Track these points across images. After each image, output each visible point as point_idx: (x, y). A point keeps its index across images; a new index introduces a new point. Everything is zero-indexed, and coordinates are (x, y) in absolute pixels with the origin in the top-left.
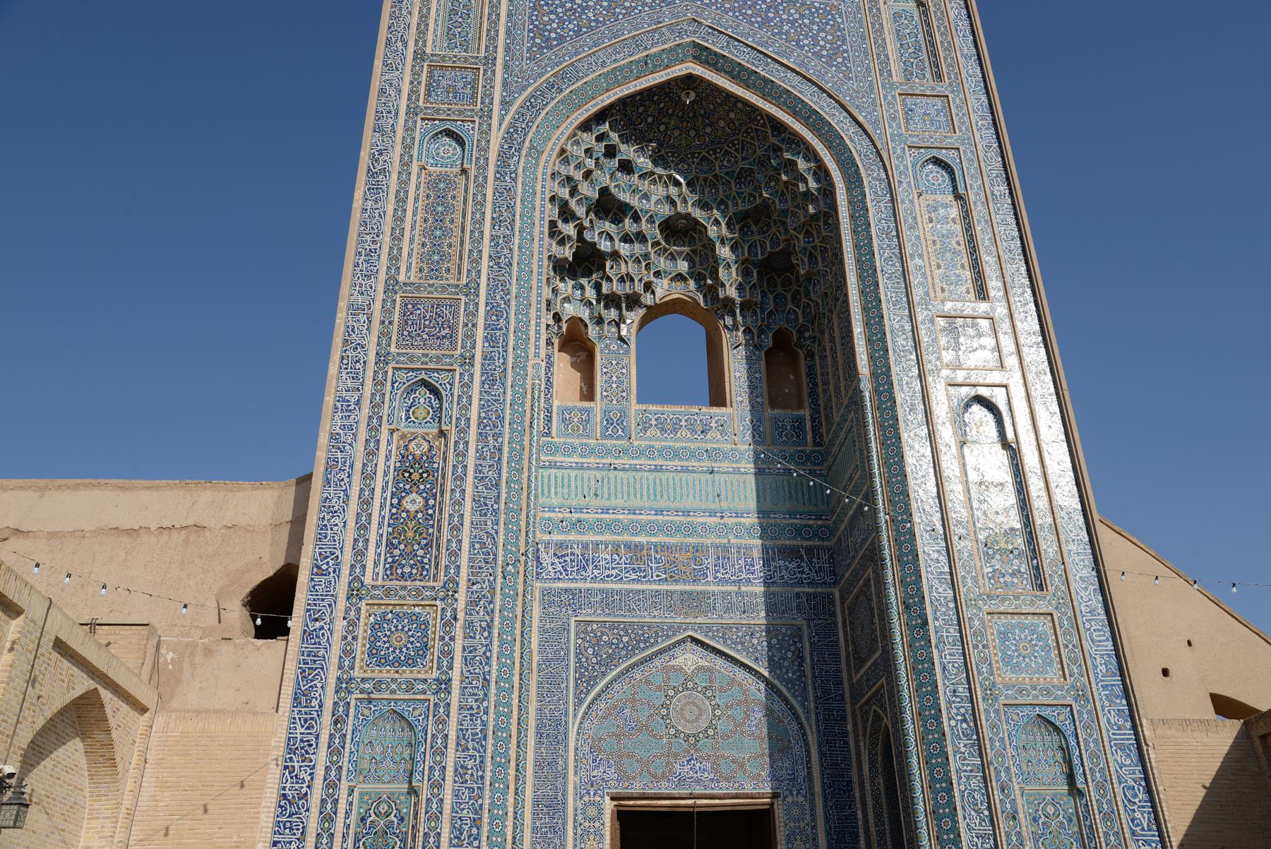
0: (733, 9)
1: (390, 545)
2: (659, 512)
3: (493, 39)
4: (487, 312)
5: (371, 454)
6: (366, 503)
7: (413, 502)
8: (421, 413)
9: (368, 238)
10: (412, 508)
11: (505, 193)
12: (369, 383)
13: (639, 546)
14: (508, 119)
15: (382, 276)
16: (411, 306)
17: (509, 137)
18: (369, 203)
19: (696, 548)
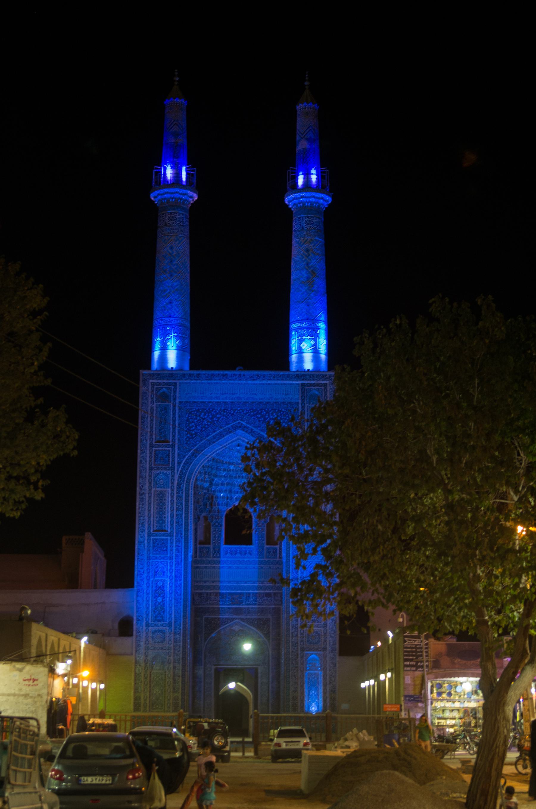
0: (254, 415)
1: (155, 612)
2: (230, 582)
3: (174, 436)
4: (176, 541)
5: (148, 587)
6: (148, 601)
7: (160, 599)
8: (160, 573)
9: (141, 518)
10: (159, 601)
11: (179, 498)
12: (146, 566)
13: (223, 594)
14: (180, 469)
15: (146, 531)
16: (155, 541)
17: (180, 477)
18: (141, 505)
19: (240, 594)
